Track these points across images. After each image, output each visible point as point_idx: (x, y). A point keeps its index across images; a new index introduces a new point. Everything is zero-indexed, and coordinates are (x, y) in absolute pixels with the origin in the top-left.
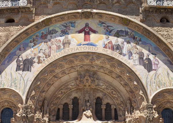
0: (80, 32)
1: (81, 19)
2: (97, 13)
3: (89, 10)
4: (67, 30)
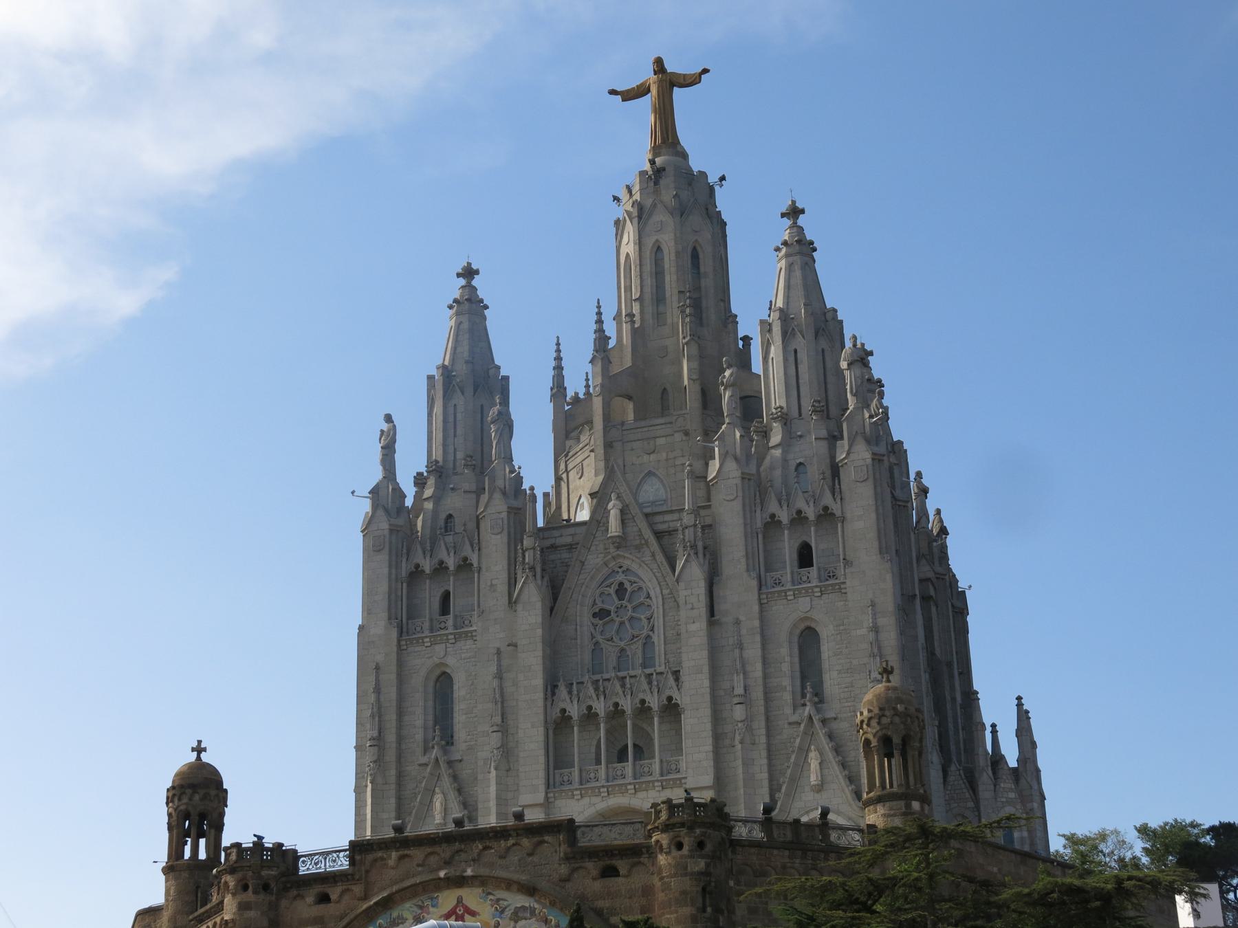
4: (425, 915)
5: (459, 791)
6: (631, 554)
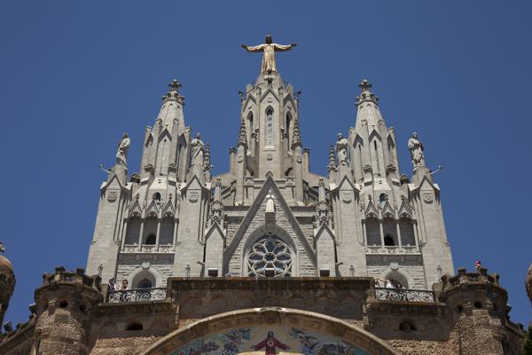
0: (258, 348)
1: (261, 323)
2: (287, 314)
3: (274, 309)
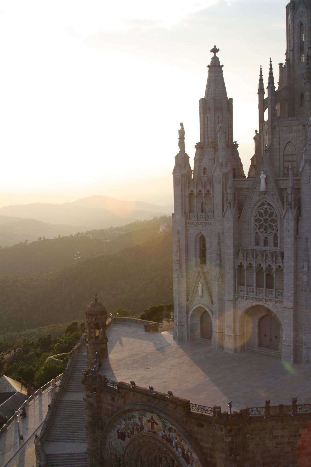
5: (207, 284)
6: (269, 197)
